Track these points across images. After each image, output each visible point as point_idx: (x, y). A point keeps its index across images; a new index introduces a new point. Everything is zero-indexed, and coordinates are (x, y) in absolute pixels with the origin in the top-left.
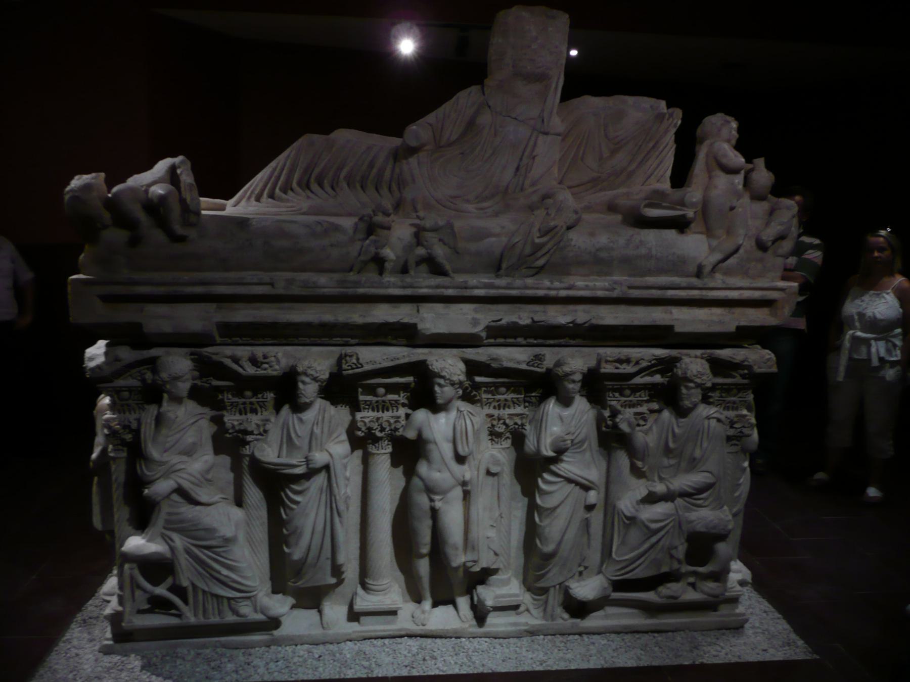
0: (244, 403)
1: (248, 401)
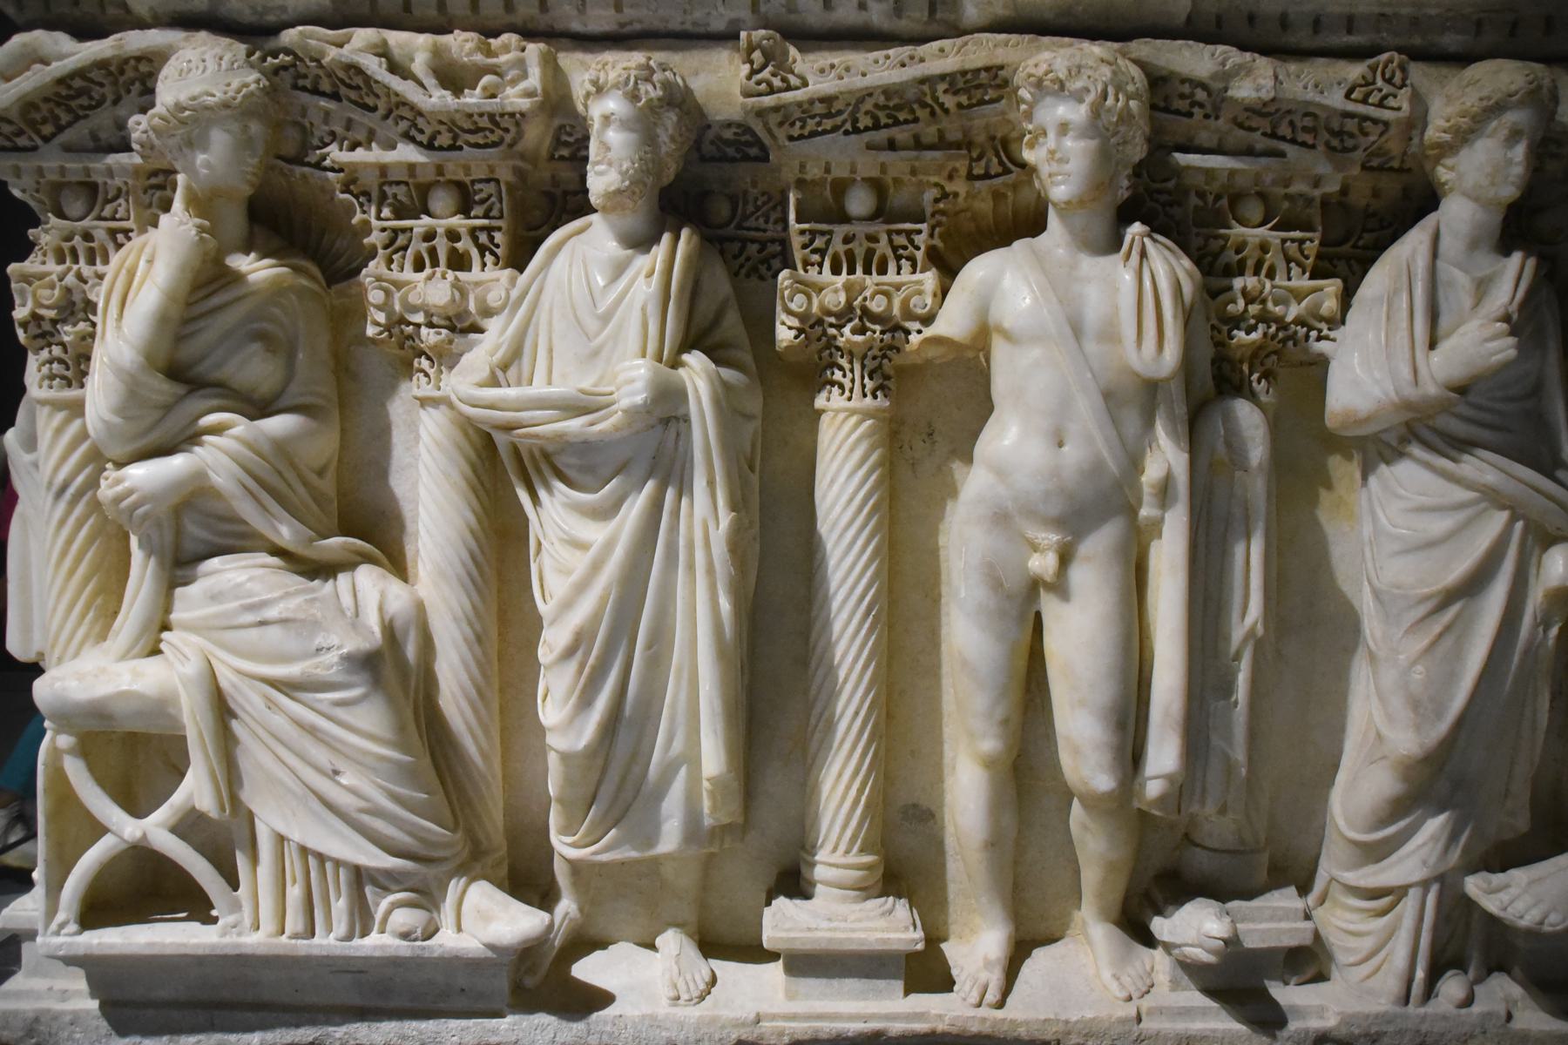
0: (429, 236)
1: (441, 225)
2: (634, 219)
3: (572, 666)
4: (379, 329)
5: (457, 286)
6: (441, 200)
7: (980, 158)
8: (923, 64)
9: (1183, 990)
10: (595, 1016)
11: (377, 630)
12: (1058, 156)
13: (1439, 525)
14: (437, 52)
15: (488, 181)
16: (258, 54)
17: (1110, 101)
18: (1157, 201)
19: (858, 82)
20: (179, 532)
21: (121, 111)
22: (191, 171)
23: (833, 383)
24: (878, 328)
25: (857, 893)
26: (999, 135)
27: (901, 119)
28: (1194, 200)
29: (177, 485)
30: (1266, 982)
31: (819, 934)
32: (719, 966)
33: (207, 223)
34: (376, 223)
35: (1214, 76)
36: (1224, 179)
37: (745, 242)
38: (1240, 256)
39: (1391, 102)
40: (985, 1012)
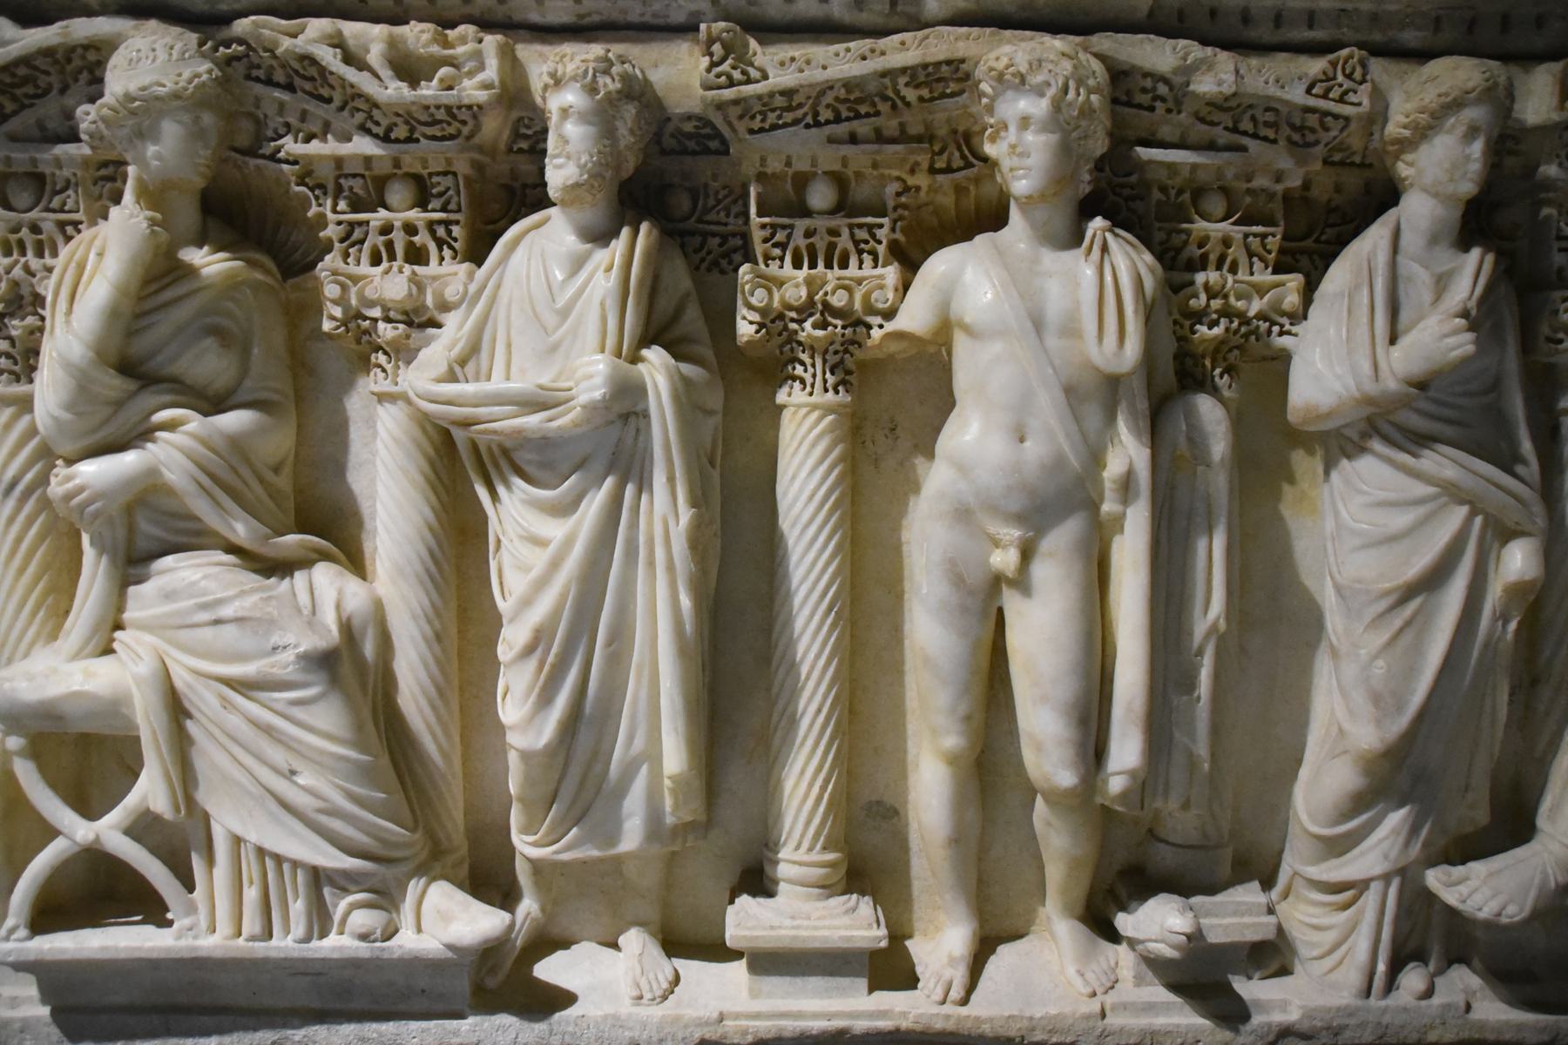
0: (386, 230)
1: (398, 218)
2: (595, 212)
3: (532, 664)
4: (335, 324)
5: (414, 280)
6: (398, 193)
7: (941, 152)
8: (882, 58)
9: (1147, 985)
10: (557, 1015)
11: (334, 629)
12: (1019, 150)
13: (1401, 520)
14: (392, 43)
15: (445, 174)
16: (209, 44)
17: (1071, 95)
18: (1119, 195)
19: (818, 76)
20: (131, 529)
21: (68, 101)
22: (142, 162)
23: (794, 378)
24: (839, 323)
25: (821, 891)
26: (961, 129)
27: (863, 112)
28: (1157, 195)
29: (128, 483)
30: (1230, 977)
31: (783, 932)
32: (681, 964)
33: (158, 216)
34: (332, 216)
35: (1176, 71)
36: (1186, 173)
37: (706, 235)
38: (1203, 250)
39: (1352, 98)
40: (949, 1009)
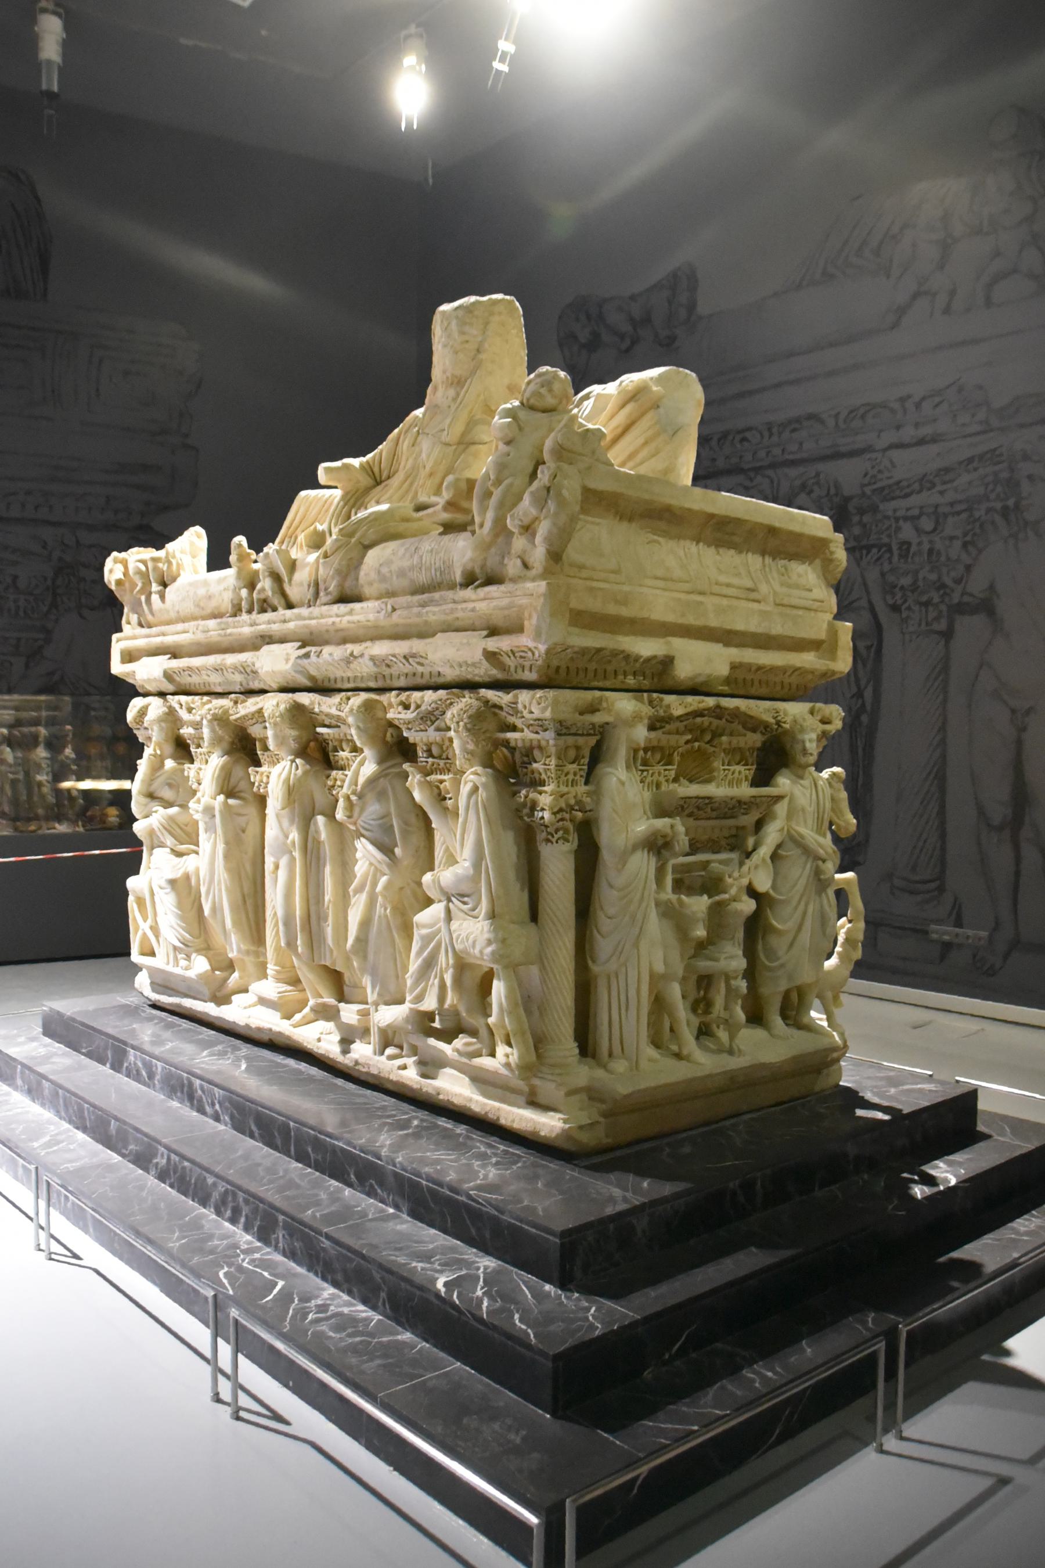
14: (187, 703)
35: (310, 704)
40: (291, 1028)
